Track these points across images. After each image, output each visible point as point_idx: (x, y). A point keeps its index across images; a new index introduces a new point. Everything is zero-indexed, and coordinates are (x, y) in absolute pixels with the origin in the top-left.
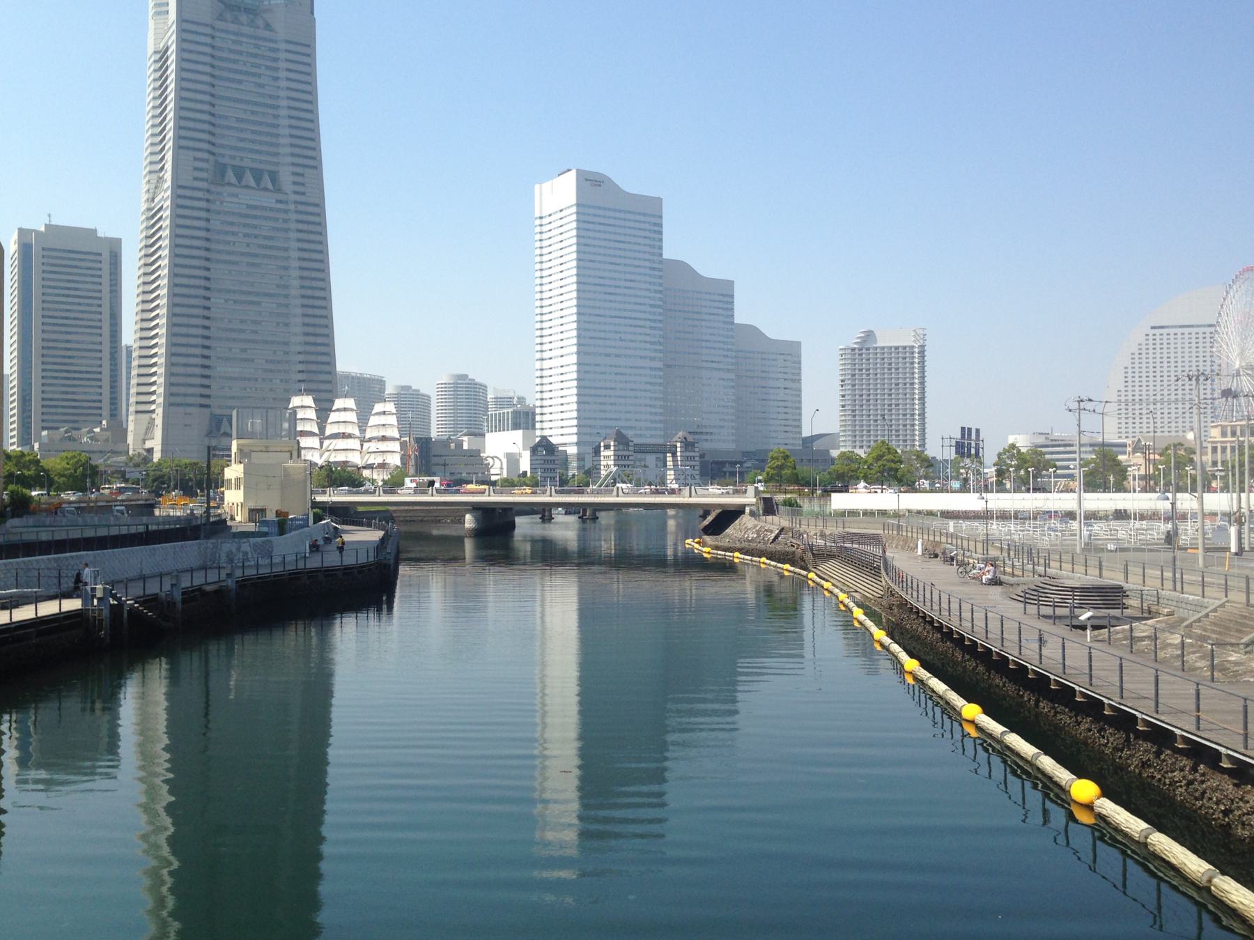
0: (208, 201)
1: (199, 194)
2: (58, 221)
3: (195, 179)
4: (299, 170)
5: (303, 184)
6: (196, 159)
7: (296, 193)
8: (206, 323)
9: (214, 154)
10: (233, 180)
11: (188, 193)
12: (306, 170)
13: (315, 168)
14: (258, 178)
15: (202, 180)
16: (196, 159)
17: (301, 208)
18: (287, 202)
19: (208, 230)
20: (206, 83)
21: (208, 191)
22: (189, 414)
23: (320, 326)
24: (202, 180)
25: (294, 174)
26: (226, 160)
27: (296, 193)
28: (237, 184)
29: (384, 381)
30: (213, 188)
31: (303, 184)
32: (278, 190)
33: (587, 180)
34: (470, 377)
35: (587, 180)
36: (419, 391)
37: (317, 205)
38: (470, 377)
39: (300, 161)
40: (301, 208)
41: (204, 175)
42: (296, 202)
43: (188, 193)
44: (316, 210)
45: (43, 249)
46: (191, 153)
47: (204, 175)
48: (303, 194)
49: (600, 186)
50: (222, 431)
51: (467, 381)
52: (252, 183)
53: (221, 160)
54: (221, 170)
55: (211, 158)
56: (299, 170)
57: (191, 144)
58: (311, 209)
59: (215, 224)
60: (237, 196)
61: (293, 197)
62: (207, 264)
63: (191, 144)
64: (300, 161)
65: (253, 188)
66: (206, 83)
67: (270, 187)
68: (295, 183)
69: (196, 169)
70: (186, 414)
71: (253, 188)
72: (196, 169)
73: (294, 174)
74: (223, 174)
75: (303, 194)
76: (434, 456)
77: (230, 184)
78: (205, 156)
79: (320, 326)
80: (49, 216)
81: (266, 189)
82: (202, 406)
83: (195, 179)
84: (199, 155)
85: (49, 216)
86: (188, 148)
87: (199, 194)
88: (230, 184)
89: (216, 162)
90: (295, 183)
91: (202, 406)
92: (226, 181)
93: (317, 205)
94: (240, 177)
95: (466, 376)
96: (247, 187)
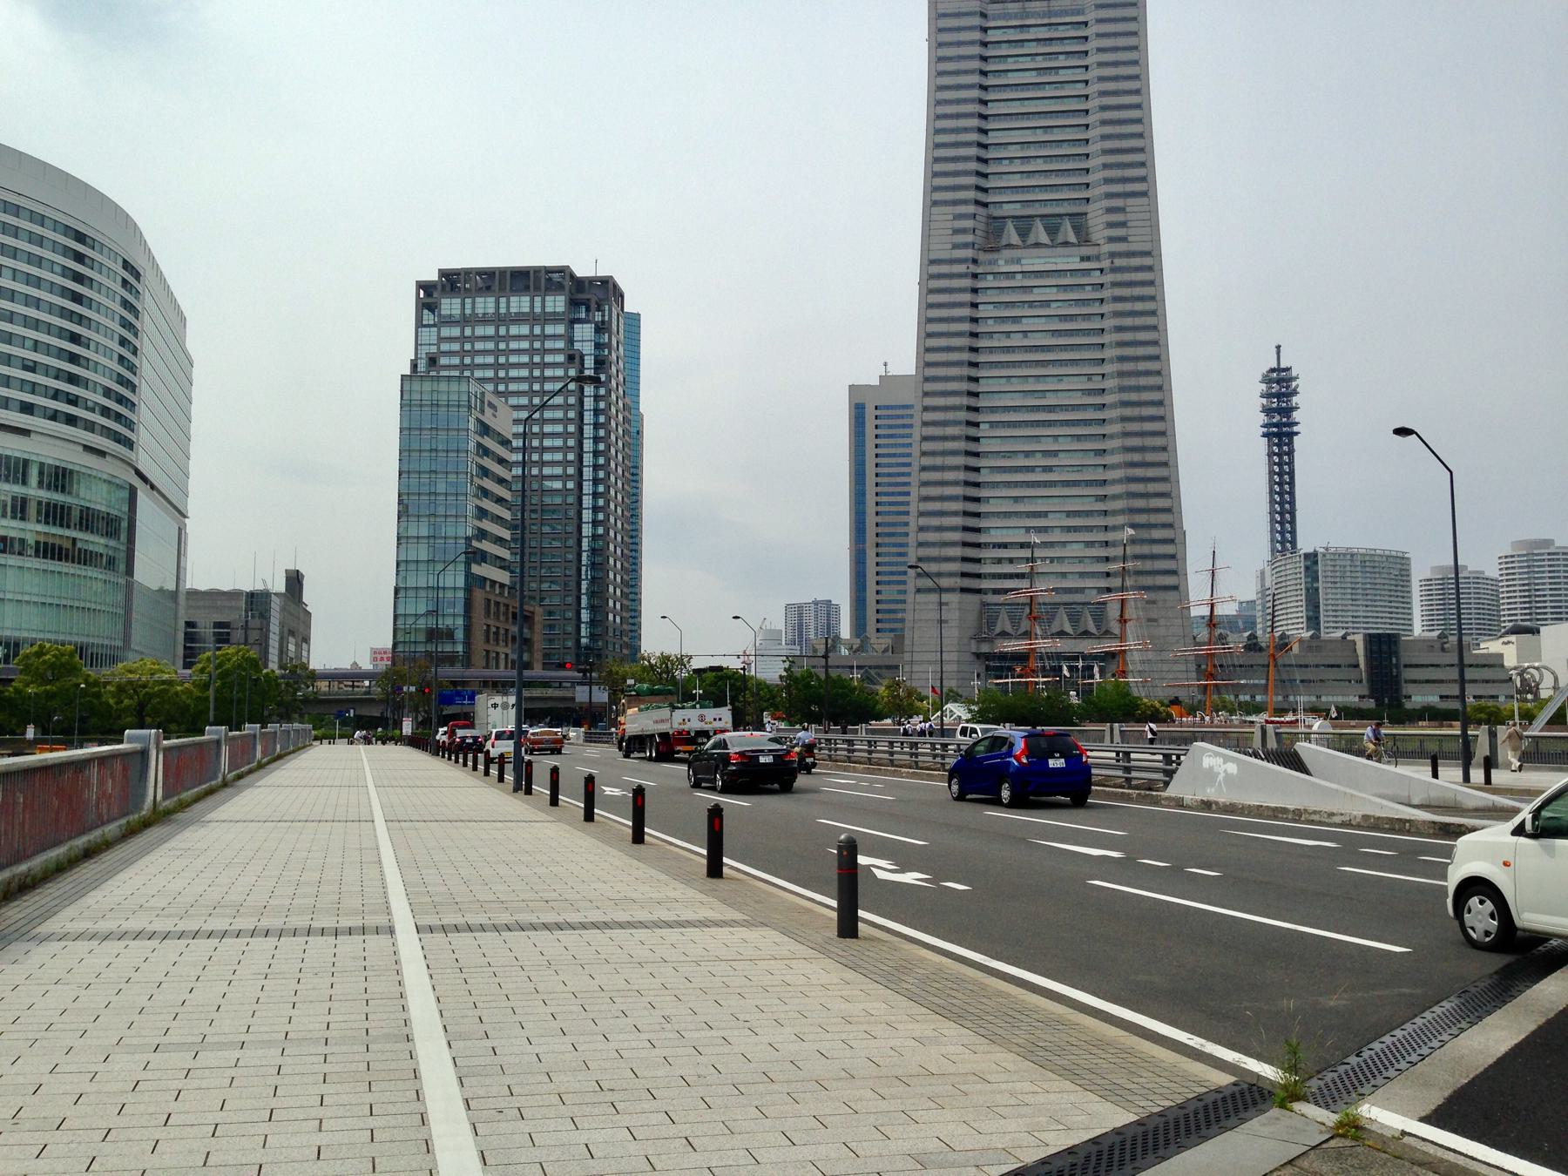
0: (975, 276)
1: (962, 268)
3: (955, 246)
4: (1119, 203)
5: (1123, 224)
6: (957, 217)
7: (1111, 240)
8: (973, 462)
9: (985, 205)
10: (1015, 239)
11: (945, 269)
12: (1130, 201)
13: (1144, 194)
14: (1052, 231)
15: (965, 246)
16: (957, 217)
17: (1118, 262)
18: (1098, 258)
19: (975, 320)
20: (972, 101)
21: (975, 261)
23: (1154, 449)
24: (965, 246)
25: (1110, 210)
26: (1008, 210)
27: (1111, 240)
28: (1020, 243)
29: (1408, 559)
30: (982, 256)
31: (1123, 224)
32: (1084, 238)
34: (1557, 544)
36: (1483, 572)
37: (1148, 254)
38: (1557, 544)
39: (1118, 188)
40: (1118, 262)
42: (1113, 255)
43: (945, 269)
44: (1147, 261)
45: (876, 408)
47: (969, 238)
48: (1123, 239)
50: (998, 630)
51: (1552, 550)
52: (1044, 238)
53: (997, 212)
54: (995, 225)
55: (981, 210)
56: (1119, 203)
57: (950, 196)
59: (983, 311)
60: (1018, 261)
61: (1107, 248)
62: (974, 372)
63: (950, 196)
64: (1118, 188)
65: (1046, 245)
66: (972, 101)
67: (1072, 238)
68: (1111, 225)
69: (956, 231)
71: (1046, 245)
72: (956, 231)
73: (1110, 210)
74: (999, 232)
75: (1123, 239)
76: (1406, 666)
77: (1009, 246)
78: (971, 209)
79: (1154, 449)
80: (885, 365)
81: (1066, 244)
82: (964, 590)
85: (885, 365)
86: (945, 203)
87: (962, 268)
88: (1009, 246)
90: (1111, 225)
91: (964, 590)
92: (1004, 242)
93: (1148, 254)
94: (1023, 234)
95: (1549, 543)
96: (1037, 245)
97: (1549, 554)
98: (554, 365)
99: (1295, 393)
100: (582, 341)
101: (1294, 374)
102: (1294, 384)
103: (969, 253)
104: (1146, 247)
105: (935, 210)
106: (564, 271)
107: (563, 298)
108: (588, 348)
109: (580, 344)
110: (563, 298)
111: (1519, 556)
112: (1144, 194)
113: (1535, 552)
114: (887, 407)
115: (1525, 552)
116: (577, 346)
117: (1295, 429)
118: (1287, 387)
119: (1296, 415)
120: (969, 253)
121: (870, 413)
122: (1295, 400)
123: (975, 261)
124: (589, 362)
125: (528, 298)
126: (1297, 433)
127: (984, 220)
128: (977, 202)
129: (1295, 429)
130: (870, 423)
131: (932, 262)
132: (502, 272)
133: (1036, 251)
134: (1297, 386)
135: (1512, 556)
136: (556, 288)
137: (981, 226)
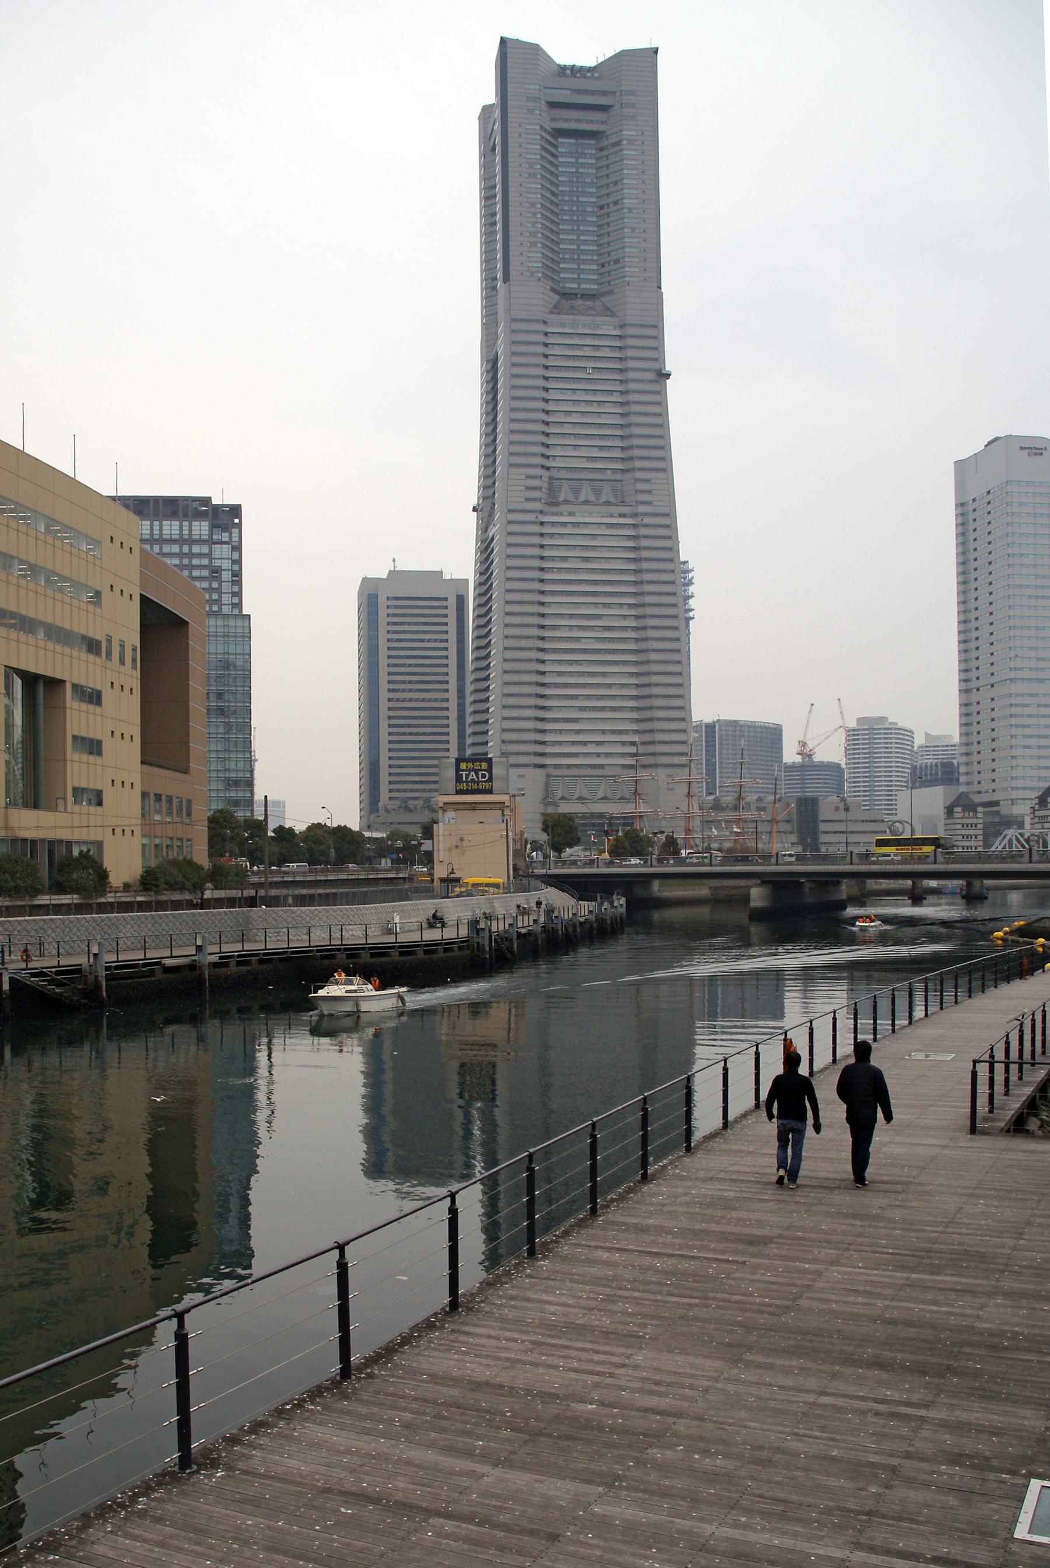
1: (531, 517)
2: (403, 566)
3: (528, 500)
9: (548, 468)
12: (654, 475)
13: (663, 470)
15: (535, 500)
16: (528, 477)
22: (523, 776)
24: (535, 500)
30: (547, 509)
33: (1022, 448)
35: (1022, 448)
37: (667, 515)
41: (537, 494)
45: (388, 599)
46: (523, 470)
47: (537, 494)
49: (1041, 454)
51: (887, 726)
53: (557, 475)
58: (659, 521)
60: (571, 514)
69: (528, 488)
70: (519, 776)
72: (528, 488)
76: (824, 821)
78: (539, 472)
83: (528, 500)
84: (531, 472)
87: (531, 517)
88: (566, 502)
89: (551, 478)
93: (667, 515)
97: (884, 729)
98: (201, 578)
99: (690, 583)
100: (221, 559)
101: (690, 567)
102: (690, 575)
103: (538, 506)
104: (666, 510)
105: (514, 470)
106: (206, 501)
107: (207, 523)
108: (226, 564)
109: (220, 561)
110: (207, 523)
111: (863, 730)
112: (663, 470)
113: (875, 727)
114: (396, 599)
115: (867, 727)
116: (217, 563)
117: (691, 614)
118: (685, 578)
119: (692, 603)
120: (538, 506)
121: (382, 601)
122: (691, 589)
123: (541, 512)
124: (226, 576)
125: (177, 523)
126: (693, 618)
127: (547, 480)
128: (543, 467)
129: (691, 614)
130: (383, 612)
131: (510, 511)
132: (156, 500)
133: (585, 508)
134: (692, 578)
135: (858, 730)
136: (200, 515)
137: (545, 485)
